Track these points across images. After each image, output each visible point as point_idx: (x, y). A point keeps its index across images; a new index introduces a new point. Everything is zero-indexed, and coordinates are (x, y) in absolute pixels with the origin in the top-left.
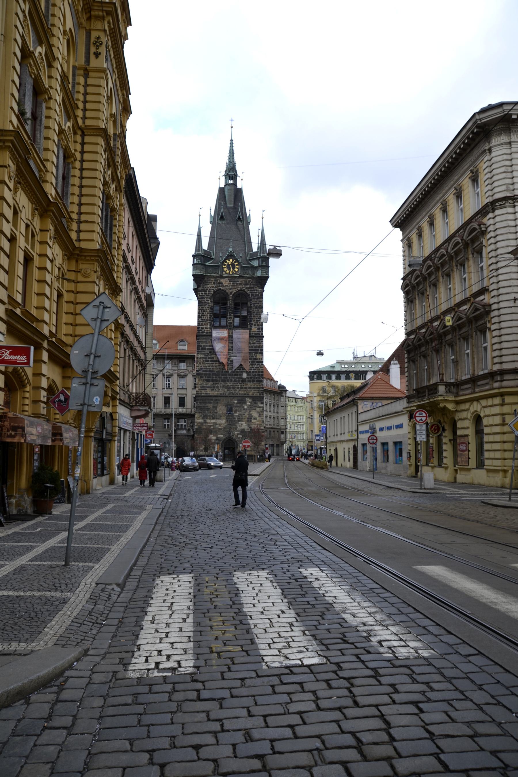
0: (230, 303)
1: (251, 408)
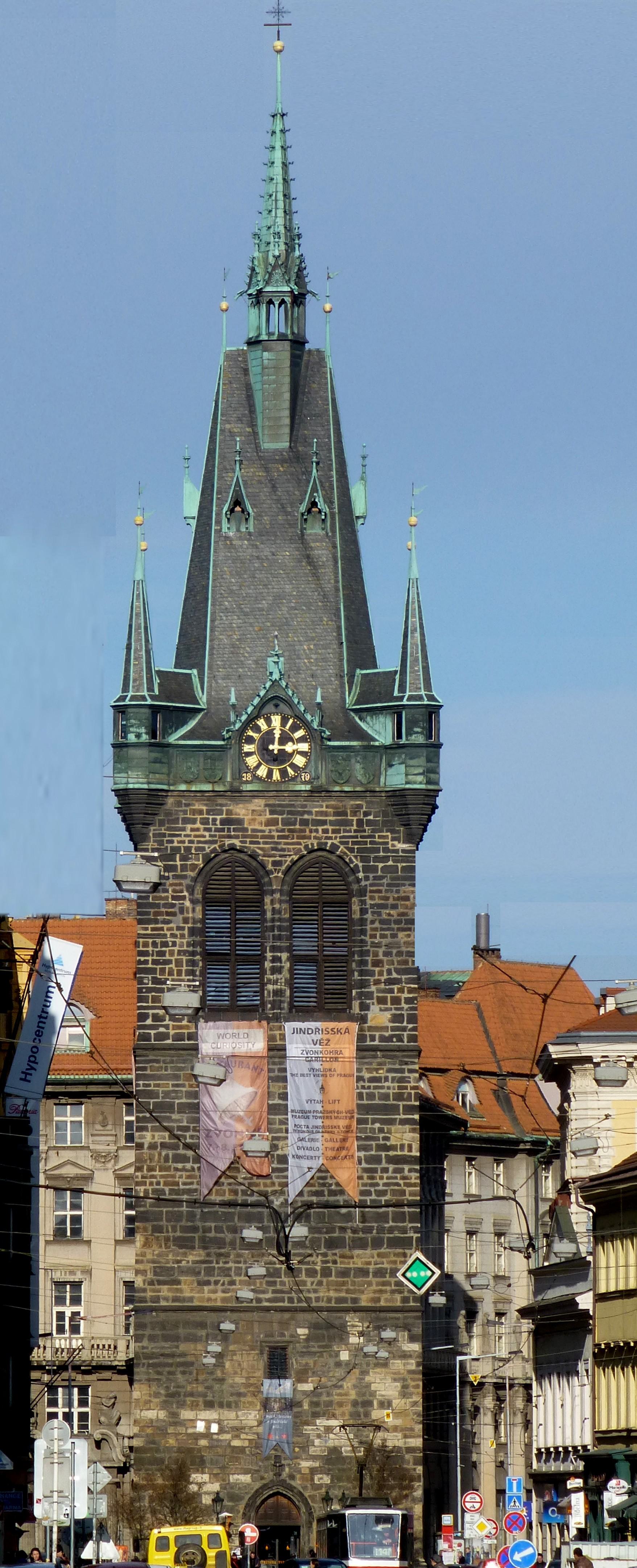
0: (274, 905)
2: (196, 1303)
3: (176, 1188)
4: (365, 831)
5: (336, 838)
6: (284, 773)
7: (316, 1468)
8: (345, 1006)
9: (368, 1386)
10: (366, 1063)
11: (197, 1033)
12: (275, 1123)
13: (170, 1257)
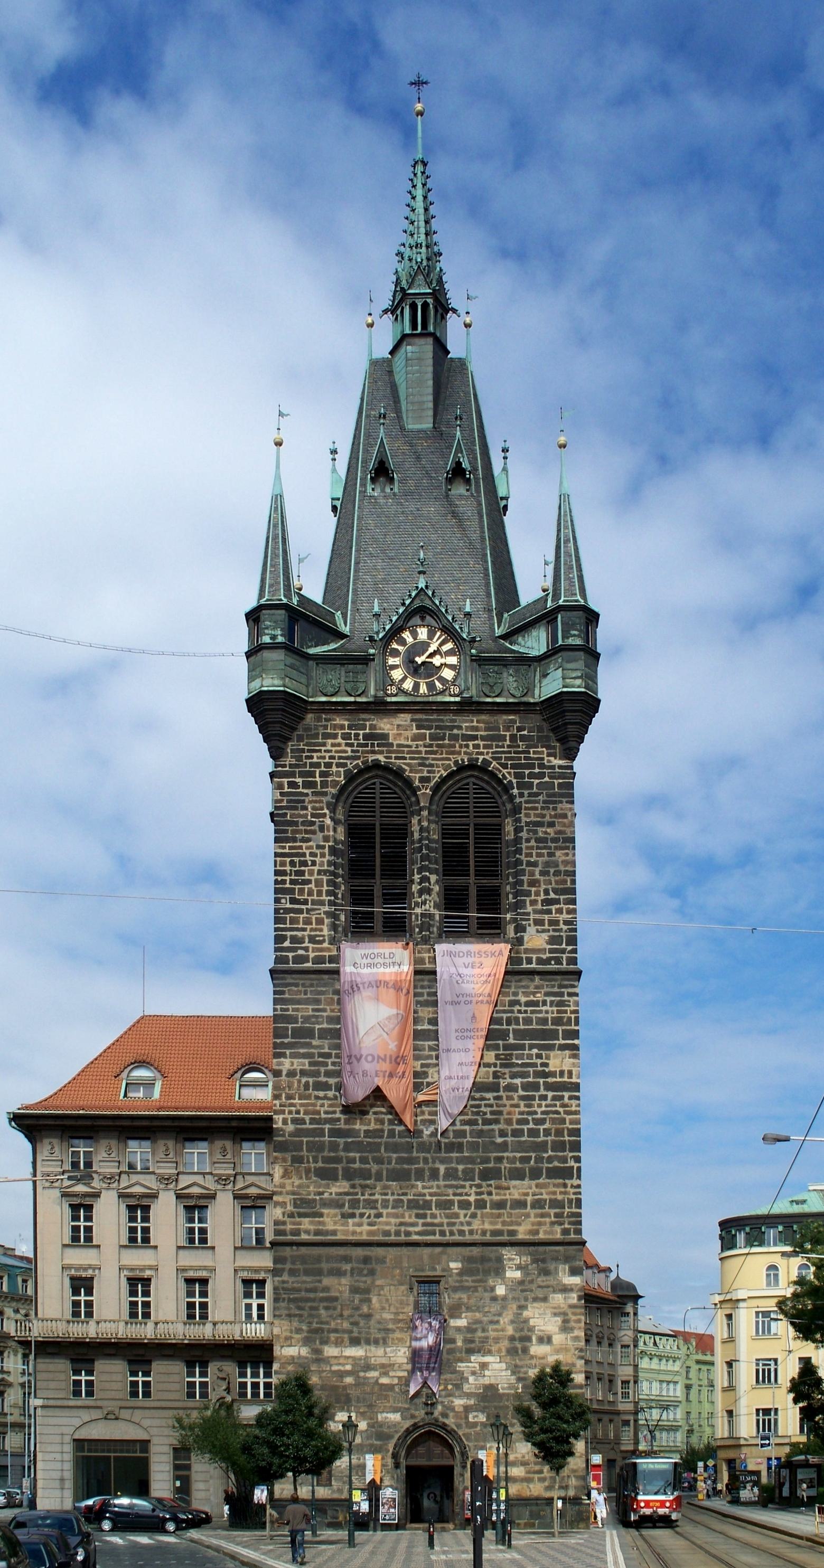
0: (423, 827)
1: (525, 1292)
2: (340, 1237)
3: (317, 1117)
4: (519, 747)
5: (488, 753)
6: (431, 686)
7: (472, 1406)
8: (499, 931)
9: (526, 1321)
10: (523, 987)
11: (339, 956)
12: (424, 1050)
13: (311, 1188)
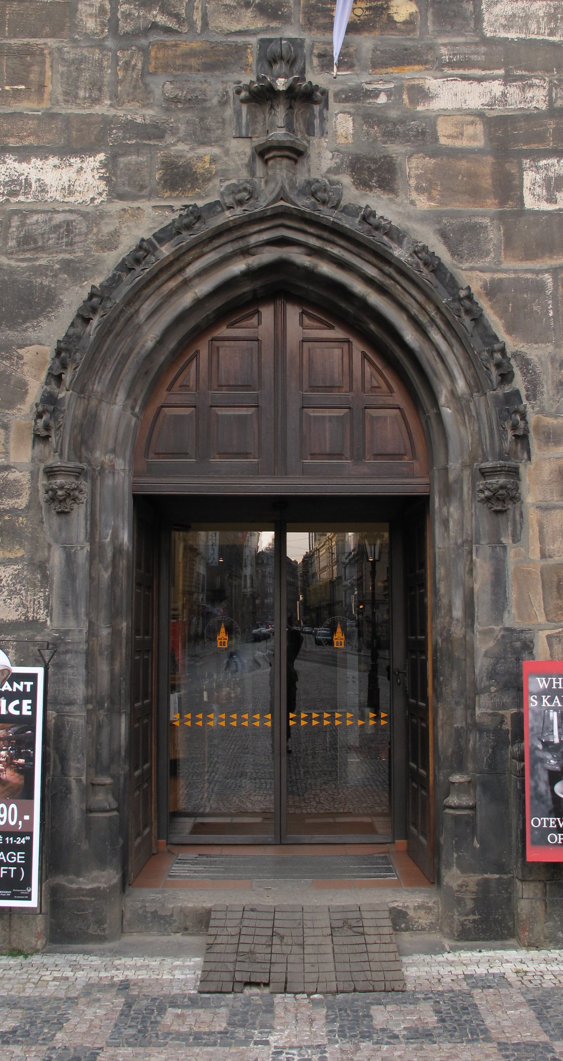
7: (529, 117)
